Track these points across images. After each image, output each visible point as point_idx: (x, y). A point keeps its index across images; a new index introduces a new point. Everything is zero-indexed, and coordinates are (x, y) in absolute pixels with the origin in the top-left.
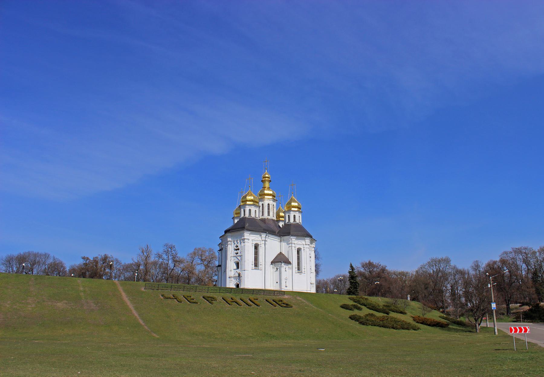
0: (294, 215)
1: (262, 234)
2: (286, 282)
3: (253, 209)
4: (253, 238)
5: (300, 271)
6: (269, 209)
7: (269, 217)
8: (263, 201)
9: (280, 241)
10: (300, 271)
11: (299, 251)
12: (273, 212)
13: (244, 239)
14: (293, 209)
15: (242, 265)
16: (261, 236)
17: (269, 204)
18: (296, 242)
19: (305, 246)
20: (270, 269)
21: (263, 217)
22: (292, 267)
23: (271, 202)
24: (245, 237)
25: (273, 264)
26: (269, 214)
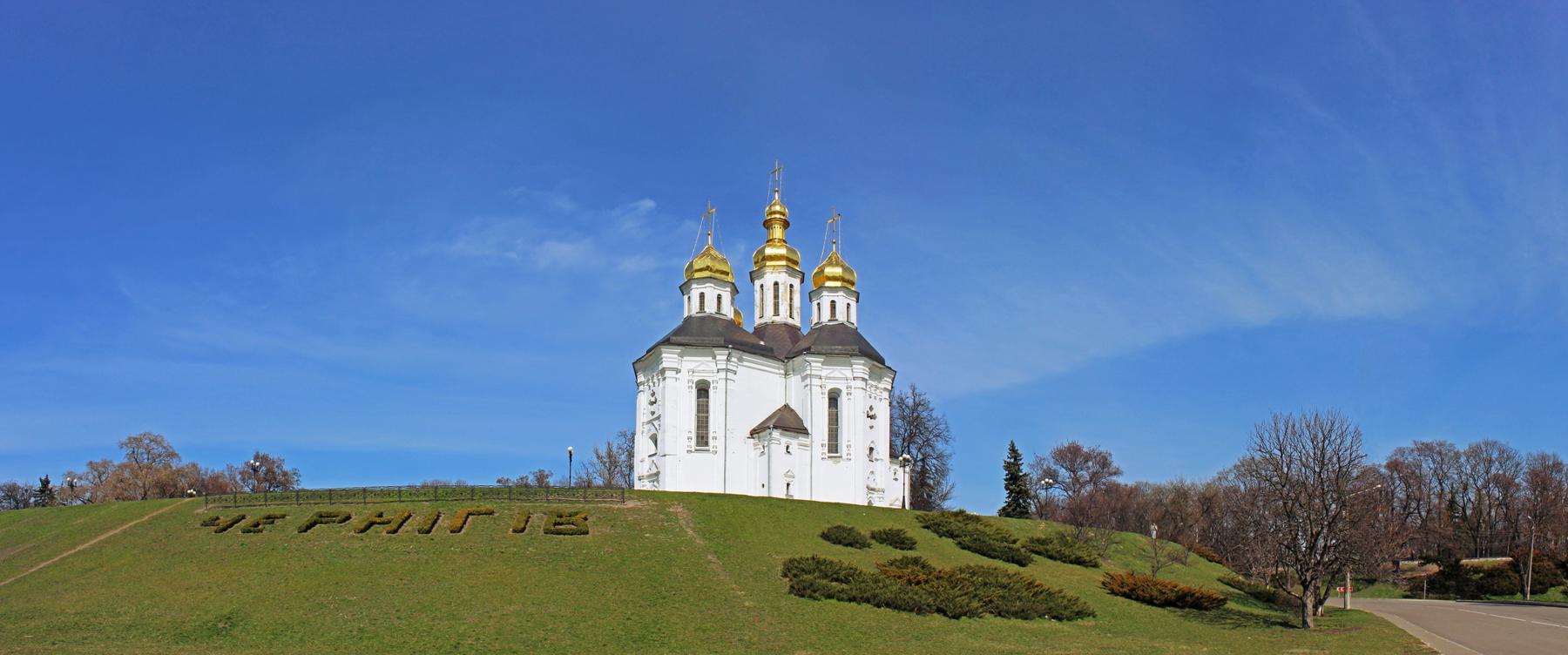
0: (833, 302)
1: (717, 351)
2: (788, 485)
3: (711, 291)
4: (692, 366)
5: (838, 455)
6: (776, 297)
7: (778, 319)
8: (761, 276)
9: (786, 374)
10: (838, 455)
11: (834, 399)
12: (791, 306)
13: (663, 371)
14: (828, 284)
15: (663, 440)
16: (714, 358)
17: (776, 284)
18: (824, 373)
19: (853, 384)
20: (746, 450)
21: (762, 321)
22: (812, 442)
23: (784, 279)
24: (664, 365)
25: (755, 435)
26: (776, 313)
